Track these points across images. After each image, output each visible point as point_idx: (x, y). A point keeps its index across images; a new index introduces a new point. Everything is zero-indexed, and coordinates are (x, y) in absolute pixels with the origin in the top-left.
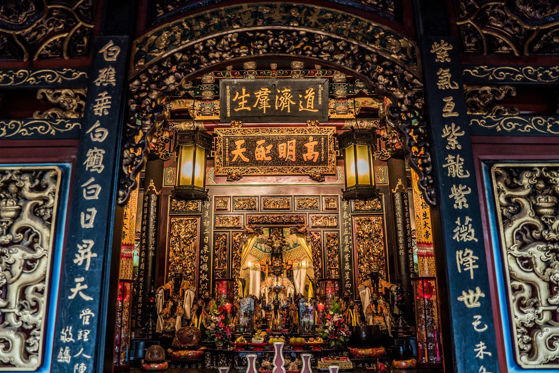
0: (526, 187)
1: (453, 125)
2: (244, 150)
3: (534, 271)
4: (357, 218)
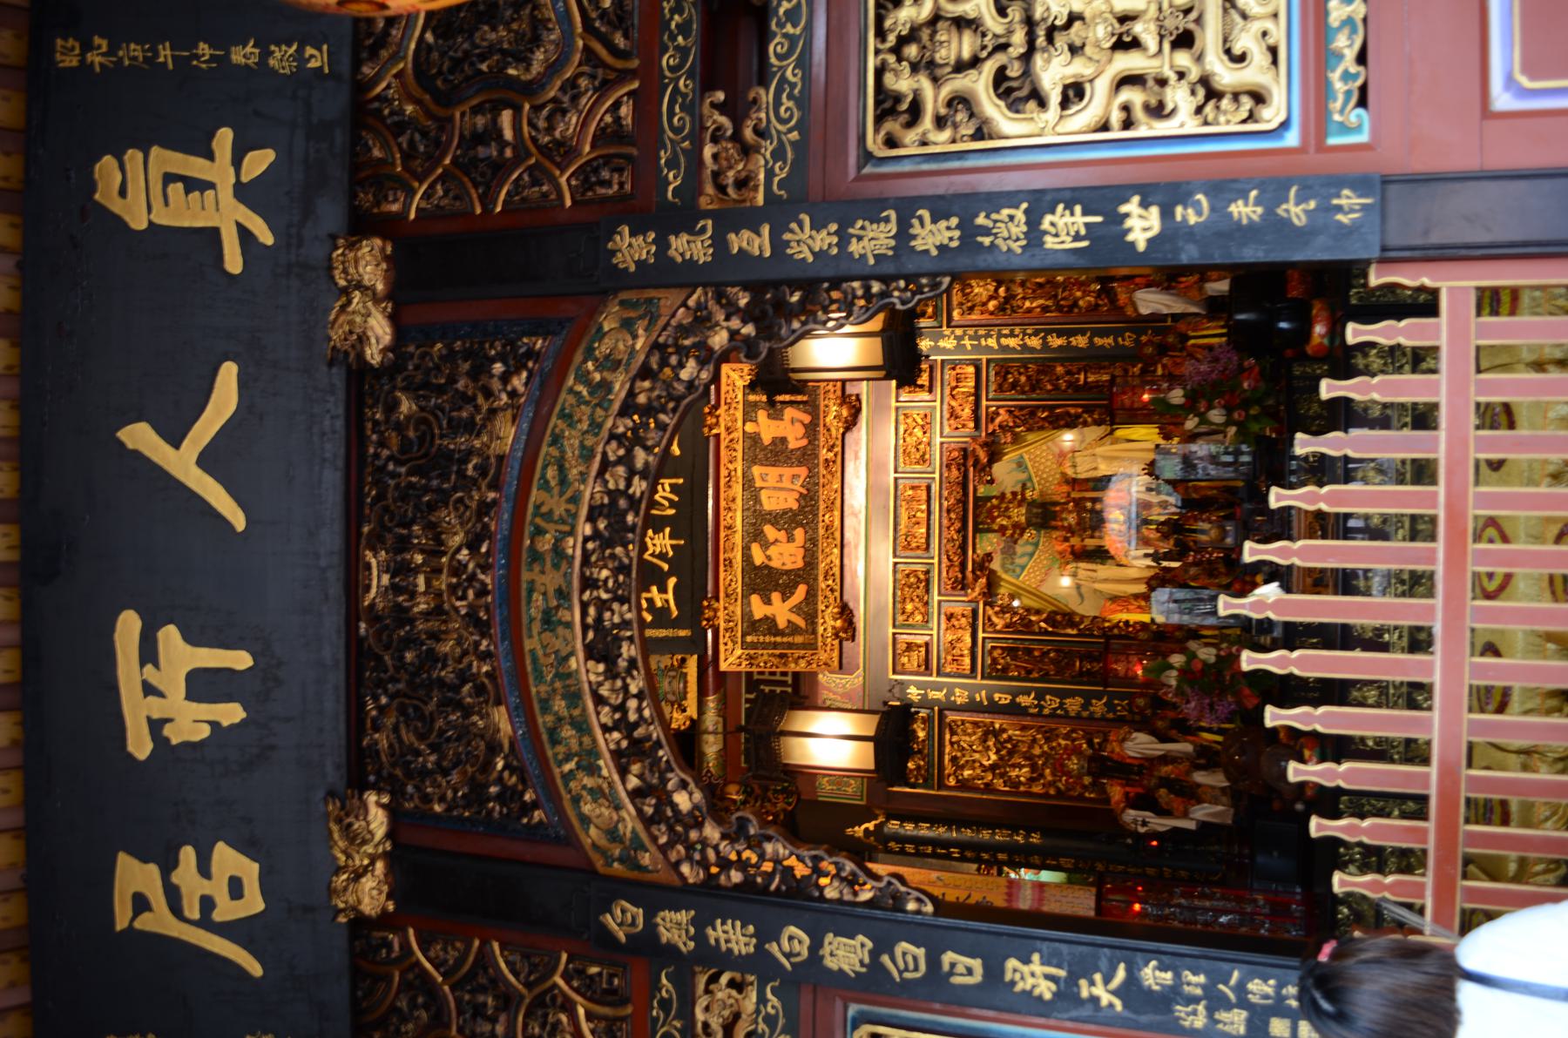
0: (915, 86)
1: (787, 236)
2: (776, 596)
3: (1091, 81)
4: (956, 314)
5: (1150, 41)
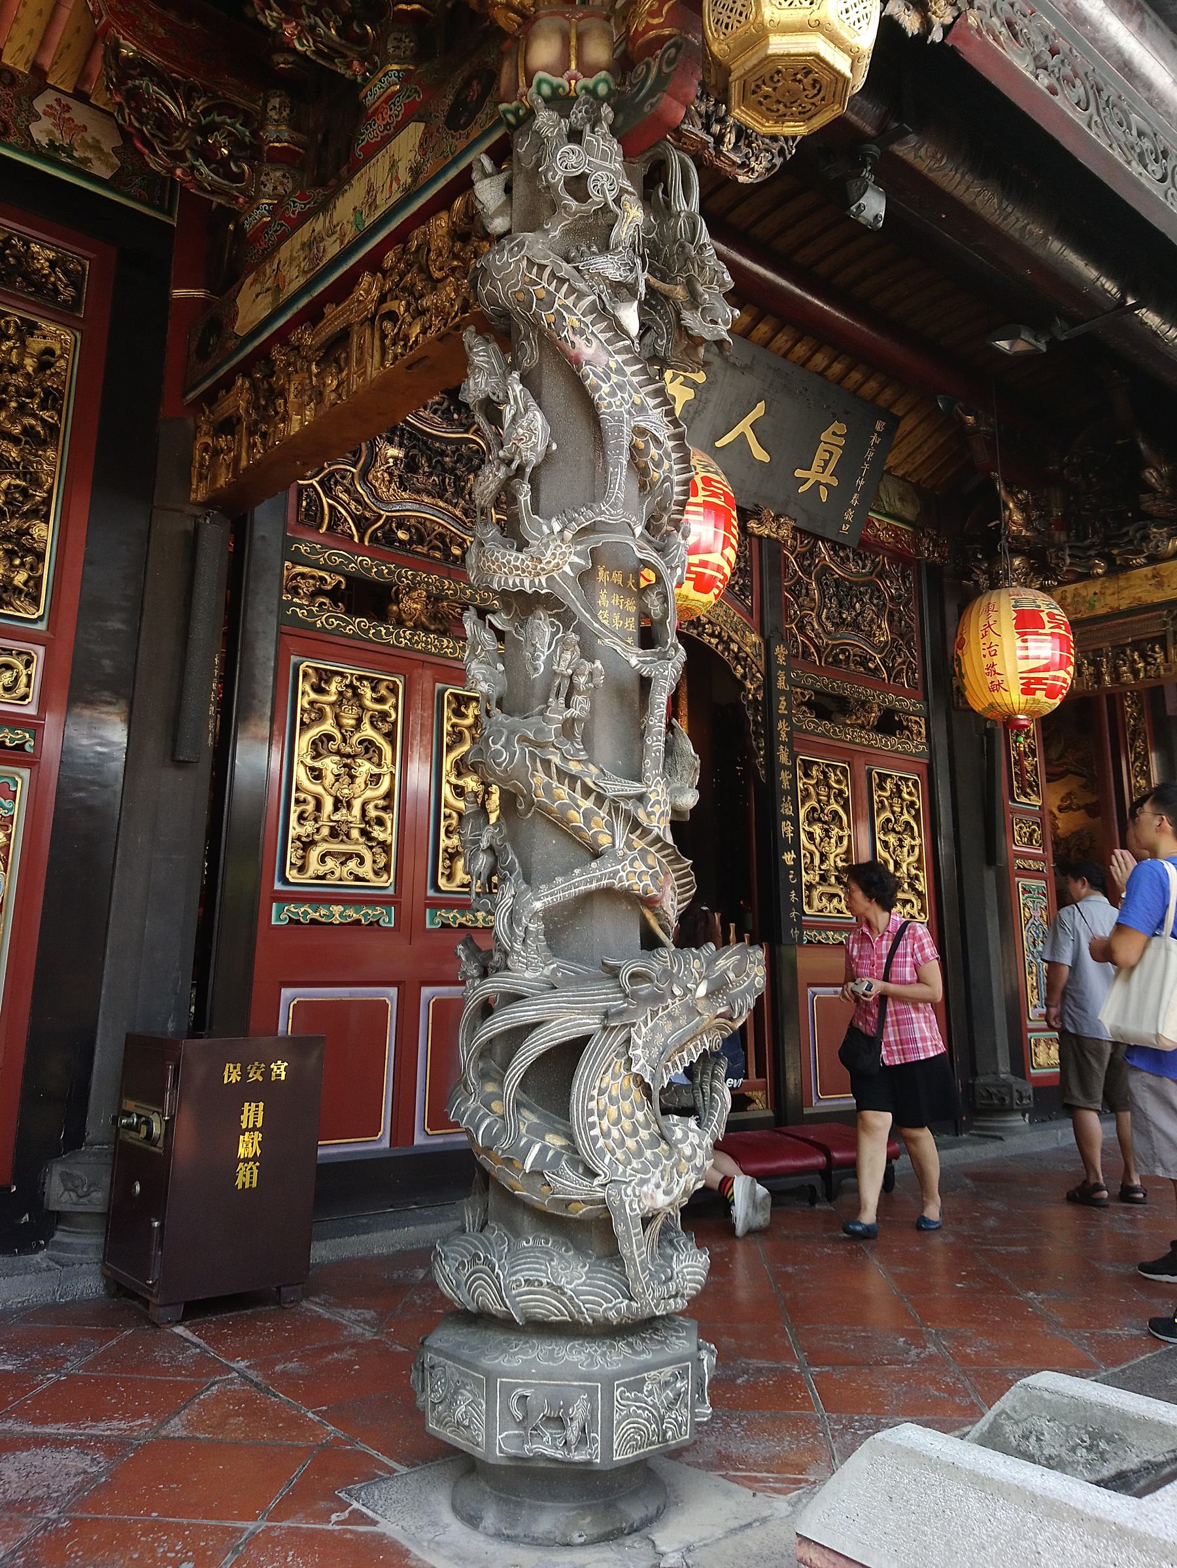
5: (335, 817)
